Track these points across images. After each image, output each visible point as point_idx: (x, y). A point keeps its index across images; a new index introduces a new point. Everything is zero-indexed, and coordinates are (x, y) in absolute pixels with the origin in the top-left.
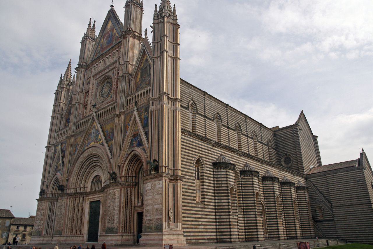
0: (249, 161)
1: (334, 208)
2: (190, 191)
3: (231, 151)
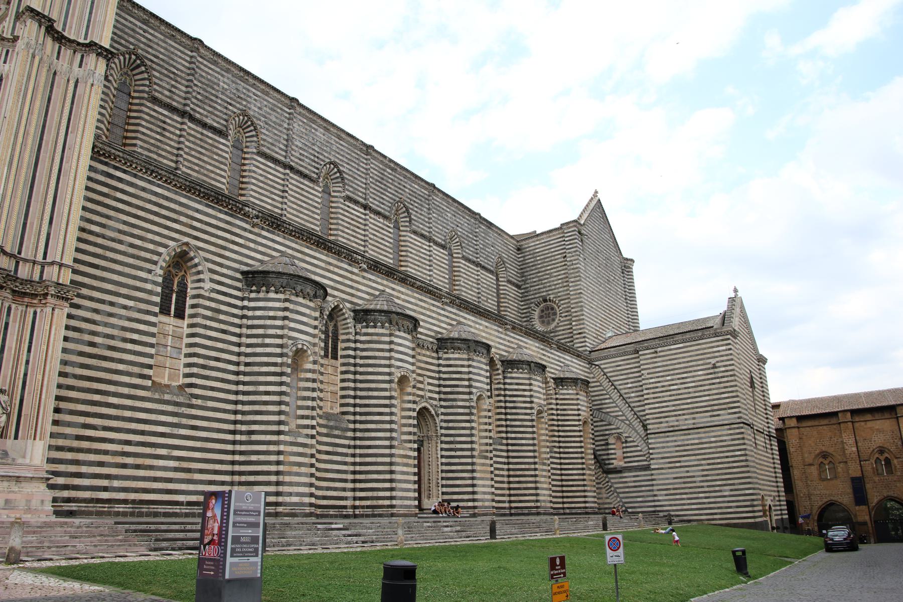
0: (393, 289)
1: (653, 436)
2: (129, 346)
3: (324, 249)
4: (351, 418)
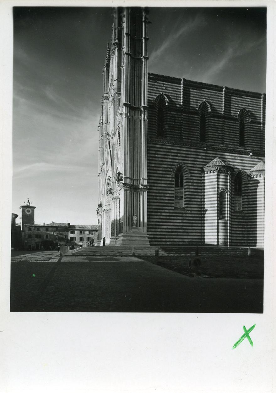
4: (246, 212)
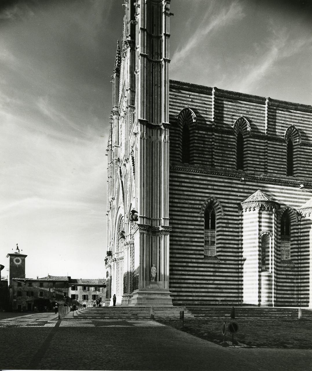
4: (296, 262)
